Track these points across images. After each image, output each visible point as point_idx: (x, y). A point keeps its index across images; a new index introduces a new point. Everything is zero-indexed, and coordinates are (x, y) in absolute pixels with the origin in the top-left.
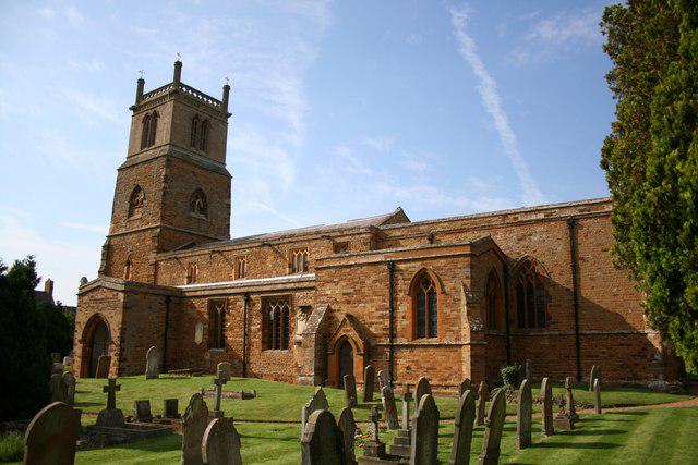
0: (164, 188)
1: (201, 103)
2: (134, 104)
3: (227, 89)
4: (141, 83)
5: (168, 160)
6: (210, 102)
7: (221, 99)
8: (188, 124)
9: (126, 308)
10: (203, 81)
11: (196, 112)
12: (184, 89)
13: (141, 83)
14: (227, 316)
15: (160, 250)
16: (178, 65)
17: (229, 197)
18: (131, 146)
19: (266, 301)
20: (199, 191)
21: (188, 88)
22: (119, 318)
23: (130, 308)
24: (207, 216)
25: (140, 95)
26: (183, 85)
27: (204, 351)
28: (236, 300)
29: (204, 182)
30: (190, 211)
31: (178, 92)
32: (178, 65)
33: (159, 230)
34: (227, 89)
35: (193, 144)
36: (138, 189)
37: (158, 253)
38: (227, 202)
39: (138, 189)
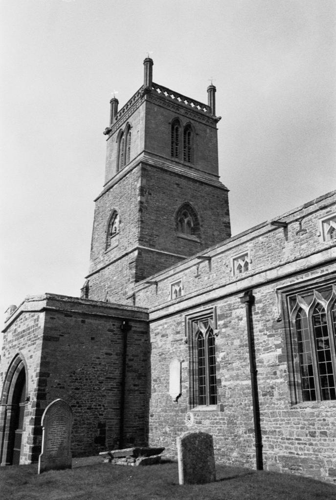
0: (141, 202)
1: (180, 106)
2: (108, 125)
3: (212, 90)
4: (115, 102)
5: (143, 169)
6: (192, 105)
7: (206, 101)
8: (166, 129)
9: (47, 339)
10: (184, 81)
11: (174, 115)
12: (159, 91)
13: (115, 102)
14: (218, 341)
15: (138, 278)
16: (149, 63)
17: (227, 214)
18: (108, 171)
19: (291, 295)
20: (186, 206)
21: (163, 89)
22: (38, 354)
23: (56, 339)
24: (200, 237)
25: (115, 112)
26: (156, 86)
27: (184, 411)
28: (231, 308)
29: (193, 196)
30: (176, 230)
31: (152, 94)
32: (149, 63)
33: (136, 253)
34: (212, 90)
35: (174, 153)
36: (114, 214)
37: (136, 281)
38: (225, 220)
39: (114, 214)
